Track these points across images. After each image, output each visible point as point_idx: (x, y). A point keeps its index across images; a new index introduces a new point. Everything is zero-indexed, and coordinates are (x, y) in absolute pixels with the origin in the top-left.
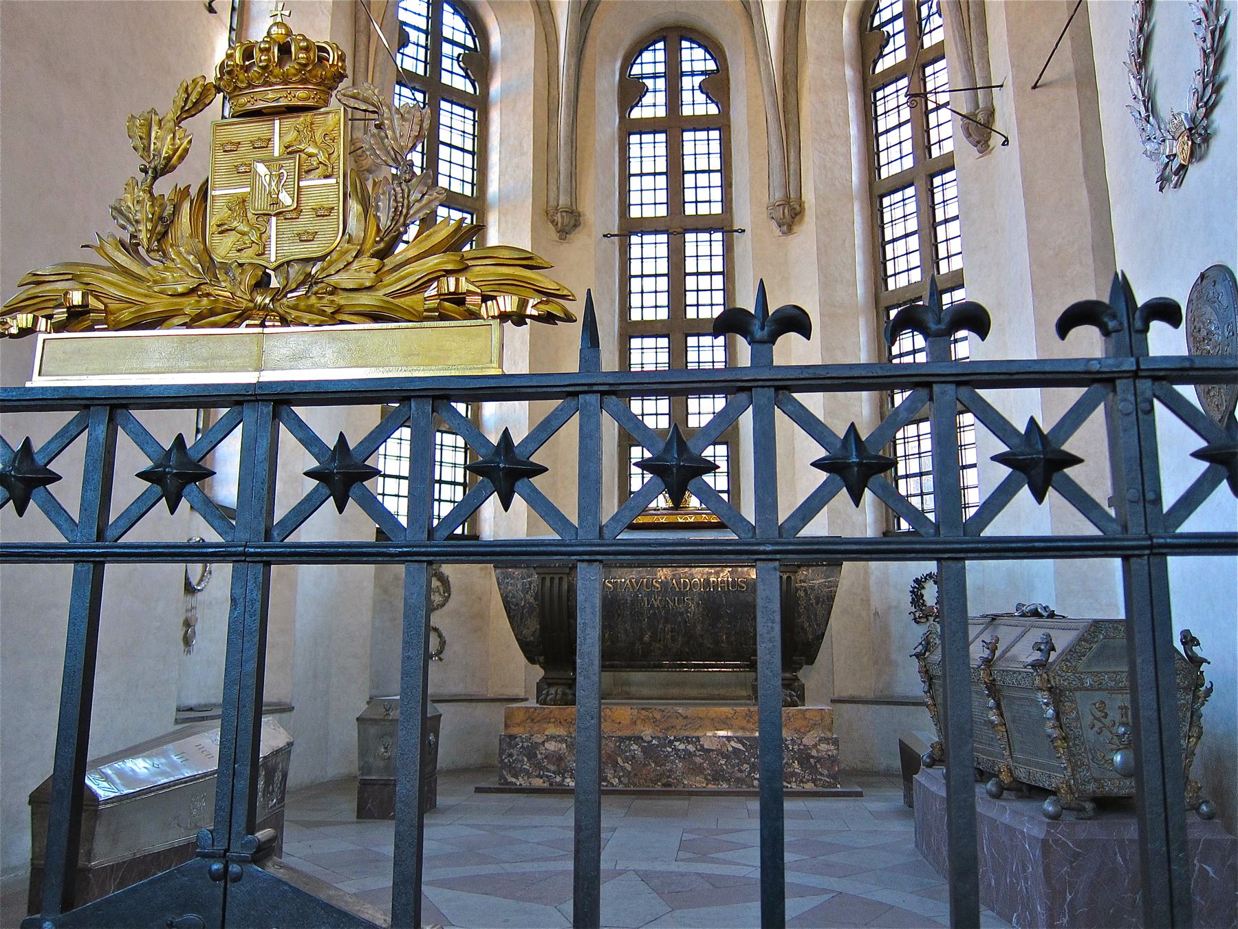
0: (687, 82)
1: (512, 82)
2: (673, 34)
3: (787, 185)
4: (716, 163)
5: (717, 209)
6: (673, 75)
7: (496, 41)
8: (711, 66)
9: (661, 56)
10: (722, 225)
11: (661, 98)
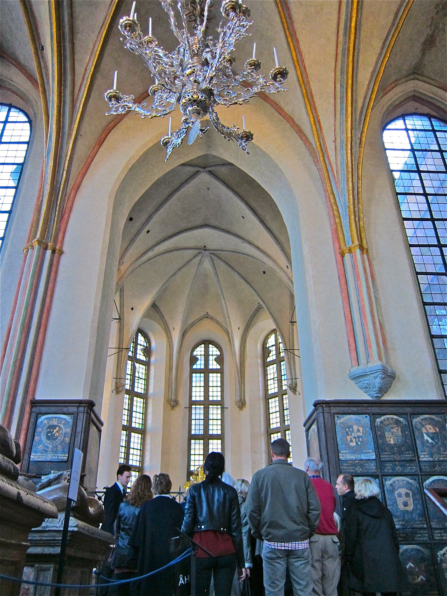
0: (211, 358)
1: (159, 357)
2: (207, 343)
3: (241, 396)
4: (219, 384)
5: (219, 399)
6: (207, 355)
7: (153, 344)
8: (218, 353)
9: (203, 349)
10: (220, 403)
11: (203, 362)
